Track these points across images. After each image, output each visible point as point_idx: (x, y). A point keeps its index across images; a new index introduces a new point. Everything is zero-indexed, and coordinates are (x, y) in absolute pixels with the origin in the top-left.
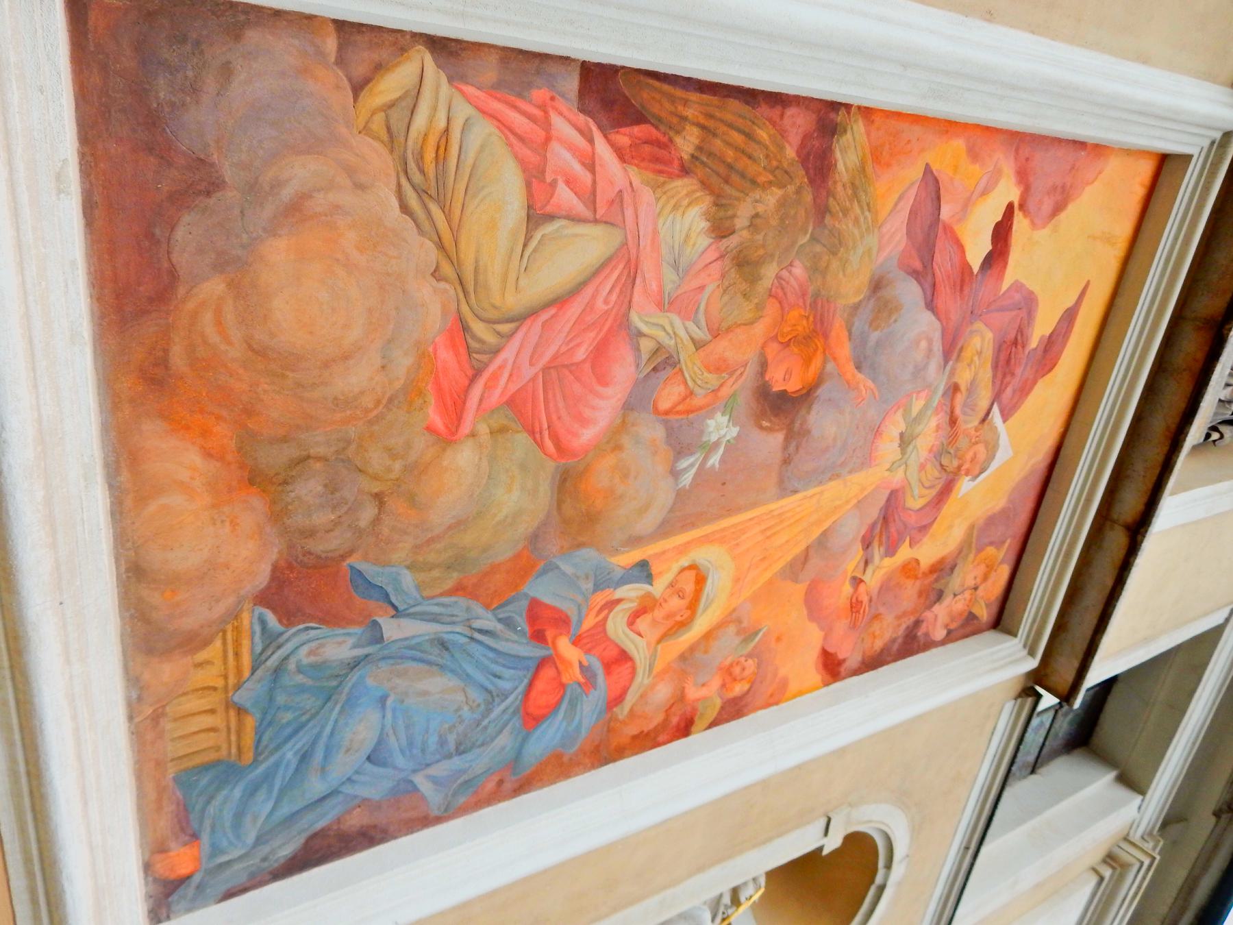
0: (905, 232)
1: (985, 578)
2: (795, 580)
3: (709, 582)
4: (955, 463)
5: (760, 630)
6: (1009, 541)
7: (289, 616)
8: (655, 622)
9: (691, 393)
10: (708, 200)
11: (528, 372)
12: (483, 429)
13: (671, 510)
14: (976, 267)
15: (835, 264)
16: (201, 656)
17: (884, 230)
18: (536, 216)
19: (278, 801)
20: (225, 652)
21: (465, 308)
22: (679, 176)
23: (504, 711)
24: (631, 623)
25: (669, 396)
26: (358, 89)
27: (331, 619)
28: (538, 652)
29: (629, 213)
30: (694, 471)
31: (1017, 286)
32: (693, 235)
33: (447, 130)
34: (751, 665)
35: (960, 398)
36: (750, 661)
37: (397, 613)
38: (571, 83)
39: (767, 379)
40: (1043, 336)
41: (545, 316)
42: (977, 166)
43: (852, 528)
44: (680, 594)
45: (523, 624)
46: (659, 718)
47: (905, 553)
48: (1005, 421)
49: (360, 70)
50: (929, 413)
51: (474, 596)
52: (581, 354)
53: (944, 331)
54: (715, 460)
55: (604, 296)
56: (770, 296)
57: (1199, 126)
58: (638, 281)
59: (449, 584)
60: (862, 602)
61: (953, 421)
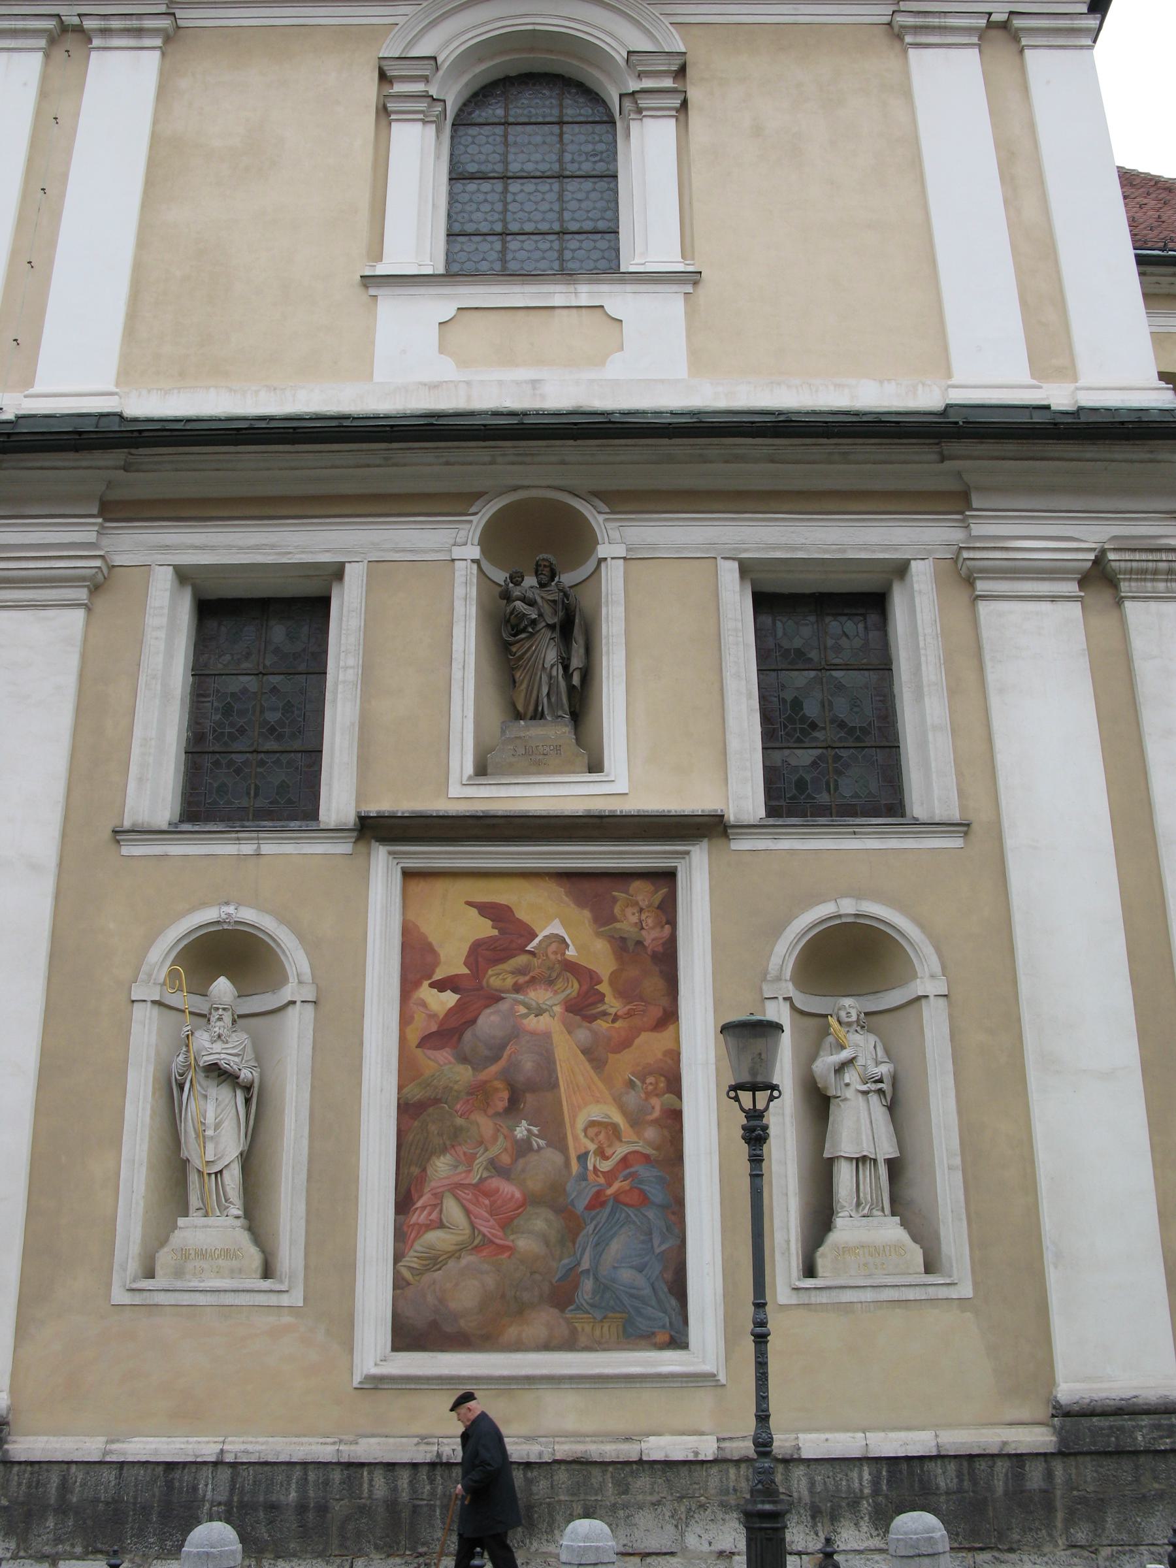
0: (441, 1051)
1: (637, 903)
2: (605, 1063)
3: (595, 1119)
4: (557, 965)
5: (630, 1079)
6: (614, 893)
7: (571, 1301)
8: (610, 1146)
9: (506, 1149)
10: (434, 1158)
11: (492, 1222)
12: (512, 1237)
13: (556, 1148)
14: (457, 997)
15: (456, 1087)
16: (580, 1329)
17: (442, 1063)
18: (441, 1225)
19: (649, 1306)
20: (580, 1322)
21: (470, 1247)
22: (426, 1172)
23: (636, 1215)
24: (607, 1158)
25: (506, 1159)
26: (409, 1284)
27: (576, 1287)
28: (610, 1203)
29: (439, 1190)
30: (538, 1140)
31: (466, 964)
32: (446, 1161)
33: (418, 1258)
34: (650, 1080)
35: (522, 980)
36: (648, 1081)
37: (579, 1264)
38: (402, 1217)
39: (501, 1111)
40: (493, 927)
41: (473, 1218)
42: (415, 1015)
43: (583, 1034)
44: (597, 1135)
45: (593, 1213)
46: (666, 1132)
47: (604, 988)
48: (537, 936)
49: (404, 1283)
50: (526, 999)
51: (577, 1235)
52: (487, 1202)
53: (487, 1006)
54: (535, 1130)
55: (467, 1195)
56: (467, 1118)
57: (388, 876)
58: (462, 1182)
59: (570, 1244)
60: (629, 1009)
61: (533, 981)
